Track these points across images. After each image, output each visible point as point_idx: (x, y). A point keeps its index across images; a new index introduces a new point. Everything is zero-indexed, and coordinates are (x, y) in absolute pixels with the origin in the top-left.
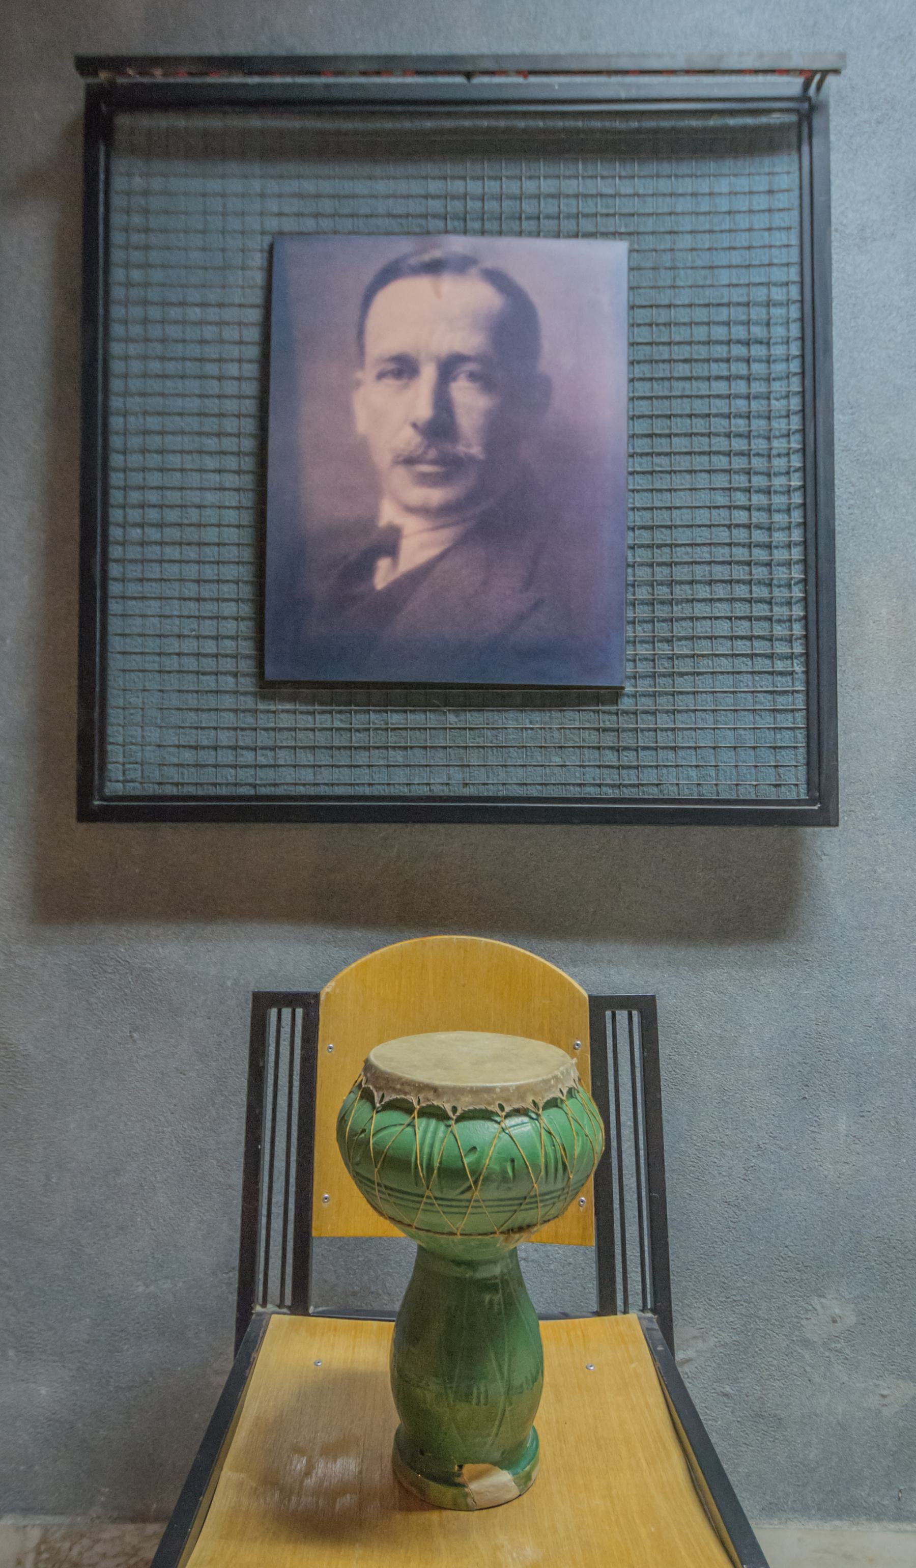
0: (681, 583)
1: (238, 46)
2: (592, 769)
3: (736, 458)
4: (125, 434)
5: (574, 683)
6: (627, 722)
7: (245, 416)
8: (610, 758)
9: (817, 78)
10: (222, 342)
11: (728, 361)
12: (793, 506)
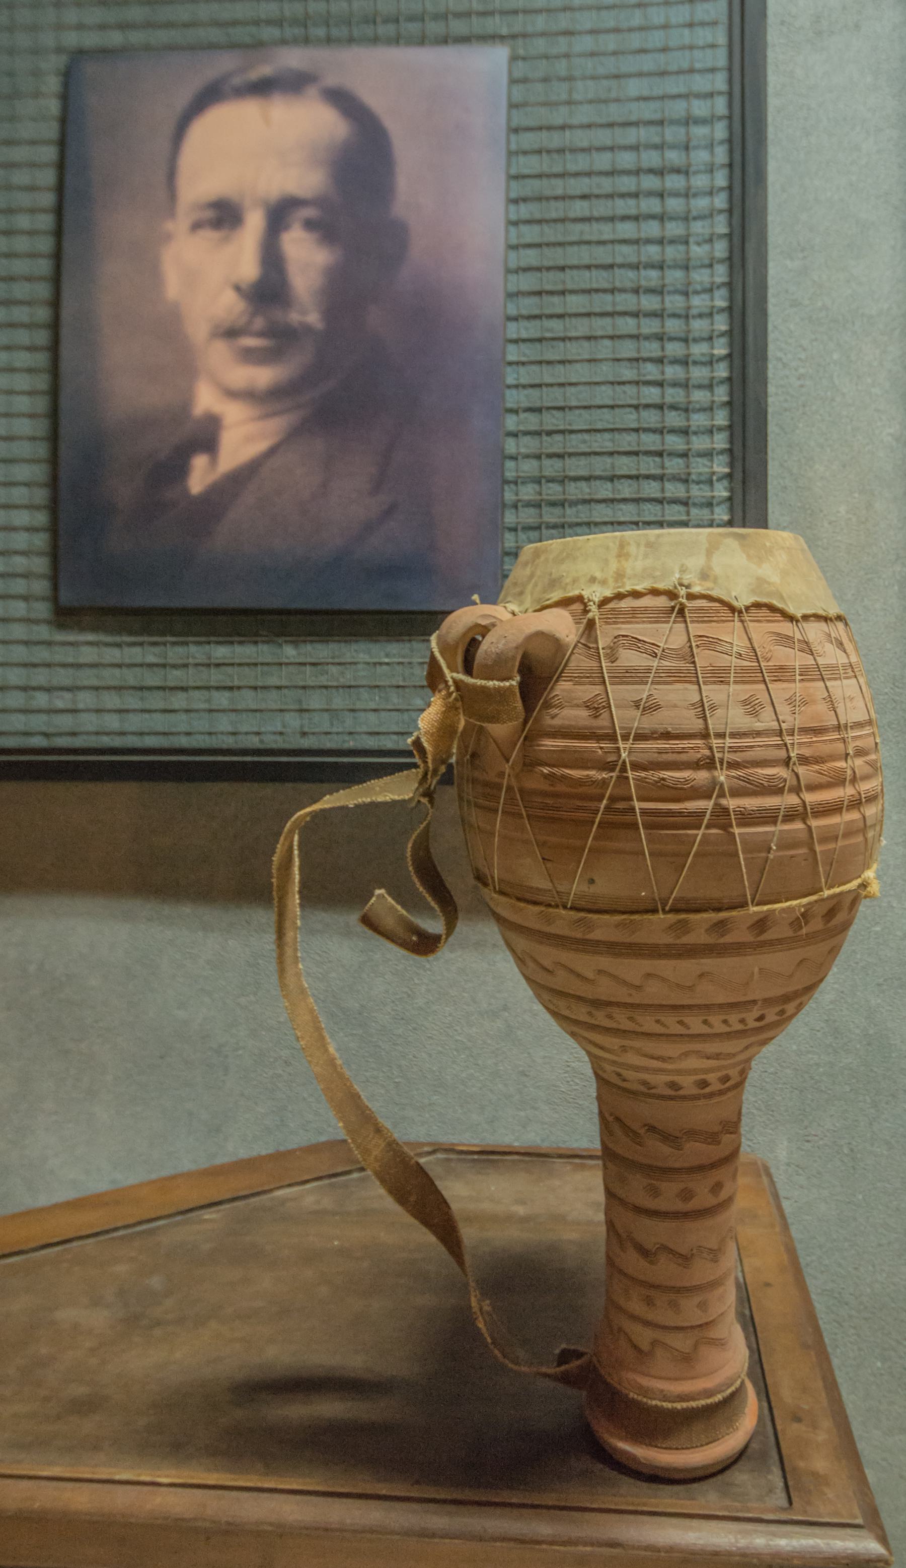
11: (636, 195)
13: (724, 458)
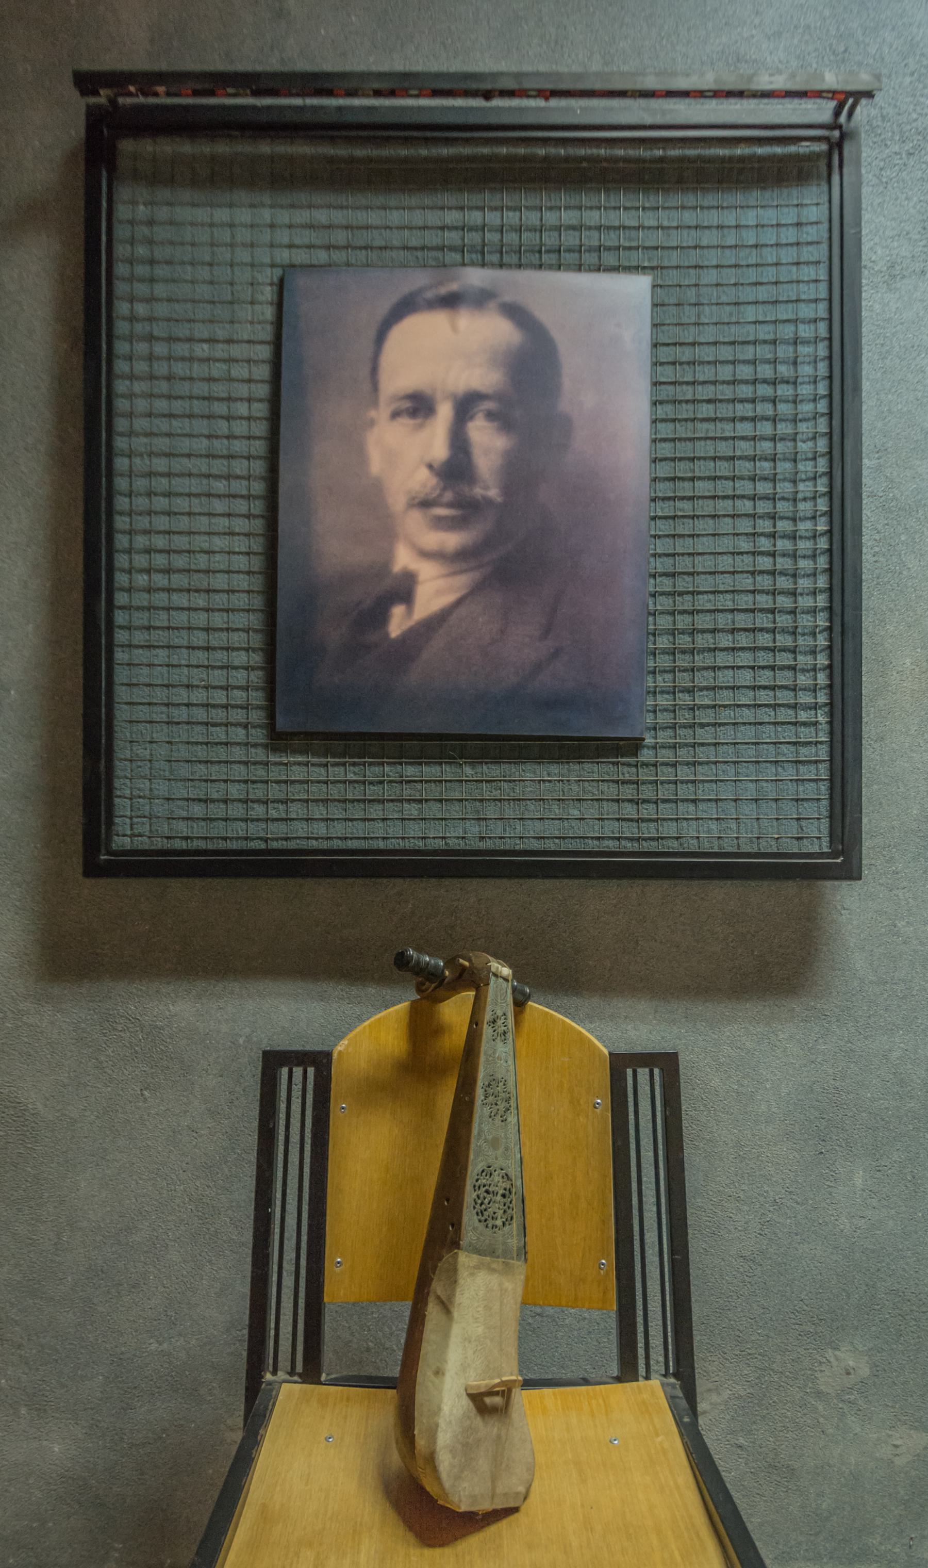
0: (703, 631)
1: (246, 62)
2: (611, 822)
3: (761, 502)
4: (130, 477)
5: (591, 734)
6: (647, 775)
7: (254, 458)
8: (629, 810)
10: (231, 380)
11: (753, 401)
12: (818, 552)
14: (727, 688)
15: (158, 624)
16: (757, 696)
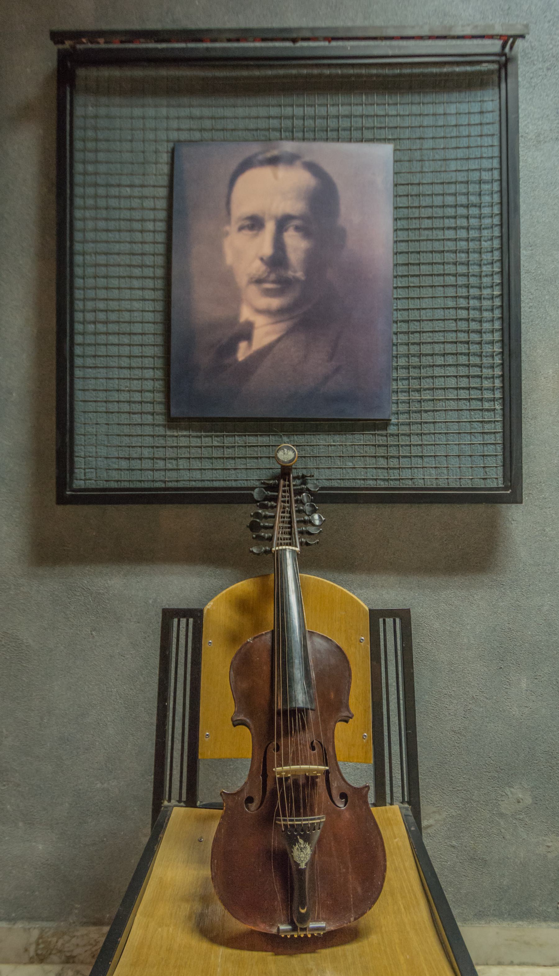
0: (426, 355)
4: (84, 266)
6: (393, 441)
7: (158, 255)
8: (382, 462)
9: (511, 40)
10: (143, 208)
11: (455, 217)
12: (495, 307)
13: (499, 345)
14: (441, 389)
15: (100, 354)
16: (459, 394)
